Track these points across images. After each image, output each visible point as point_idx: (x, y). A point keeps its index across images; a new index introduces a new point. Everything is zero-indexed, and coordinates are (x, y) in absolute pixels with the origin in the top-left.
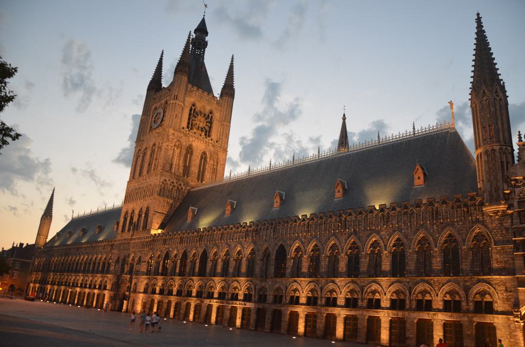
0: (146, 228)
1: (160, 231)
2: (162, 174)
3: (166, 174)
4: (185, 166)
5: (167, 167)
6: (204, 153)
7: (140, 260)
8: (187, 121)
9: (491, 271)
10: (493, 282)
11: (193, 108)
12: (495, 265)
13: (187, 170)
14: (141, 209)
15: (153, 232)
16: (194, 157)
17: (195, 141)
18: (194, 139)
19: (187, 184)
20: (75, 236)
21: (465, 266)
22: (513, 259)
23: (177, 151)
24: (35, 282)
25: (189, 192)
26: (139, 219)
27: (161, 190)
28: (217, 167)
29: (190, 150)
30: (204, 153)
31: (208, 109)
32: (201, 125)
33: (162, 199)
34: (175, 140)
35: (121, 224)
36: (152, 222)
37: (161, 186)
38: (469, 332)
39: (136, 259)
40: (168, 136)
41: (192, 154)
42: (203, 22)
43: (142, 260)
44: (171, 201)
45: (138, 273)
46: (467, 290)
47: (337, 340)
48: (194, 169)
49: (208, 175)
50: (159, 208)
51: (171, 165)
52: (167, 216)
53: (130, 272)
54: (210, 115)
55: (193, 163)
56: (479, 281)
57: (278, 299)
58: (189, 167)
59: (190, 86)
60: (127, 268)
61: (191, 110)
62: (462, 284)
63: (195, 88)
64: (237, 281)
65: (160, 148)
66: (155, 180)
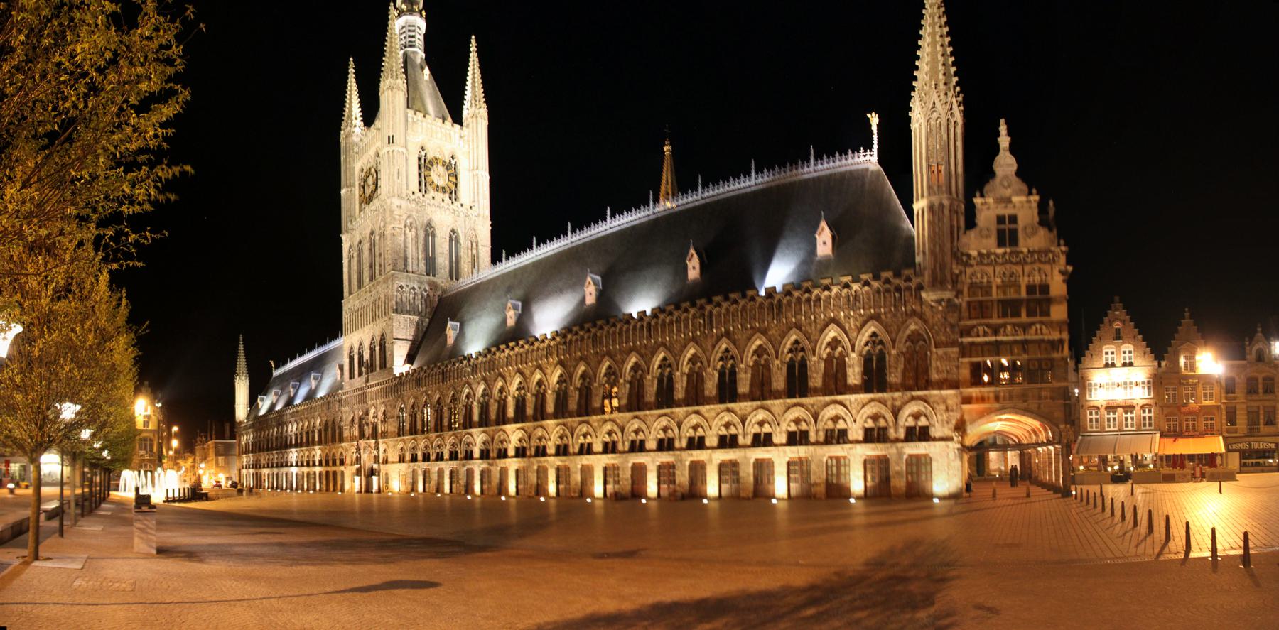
0: (385, 363)
1: (407, 368)
3: (400, 275)
5: (400, 265)
9: (928, 385)
10: (931, 400)
12: (935, 376)
15: (397, 372)
21: (894, 377)
22: (957, 367)
23: (411, 235)
25: (440, 299)
26: (371, 355)
29: (429, 231)
33: (401, 317)
34: (405, 217)
35: (346, 368)
36: (392, 355)
38: (897, 468)
39: (380, 415)
40: (392, 212)
41: (434, 235)
43: (388, 414)
44: (416, 318)
46: (896, 412)
47: (709, 499)
48: (442, 261)
49: (465, 266)
51: (406, 260)
55: (438, 250)
56: (913, 398)
58: (434, 258)
62: (889, 403)
64: (542, 427)
65: (382, 235)
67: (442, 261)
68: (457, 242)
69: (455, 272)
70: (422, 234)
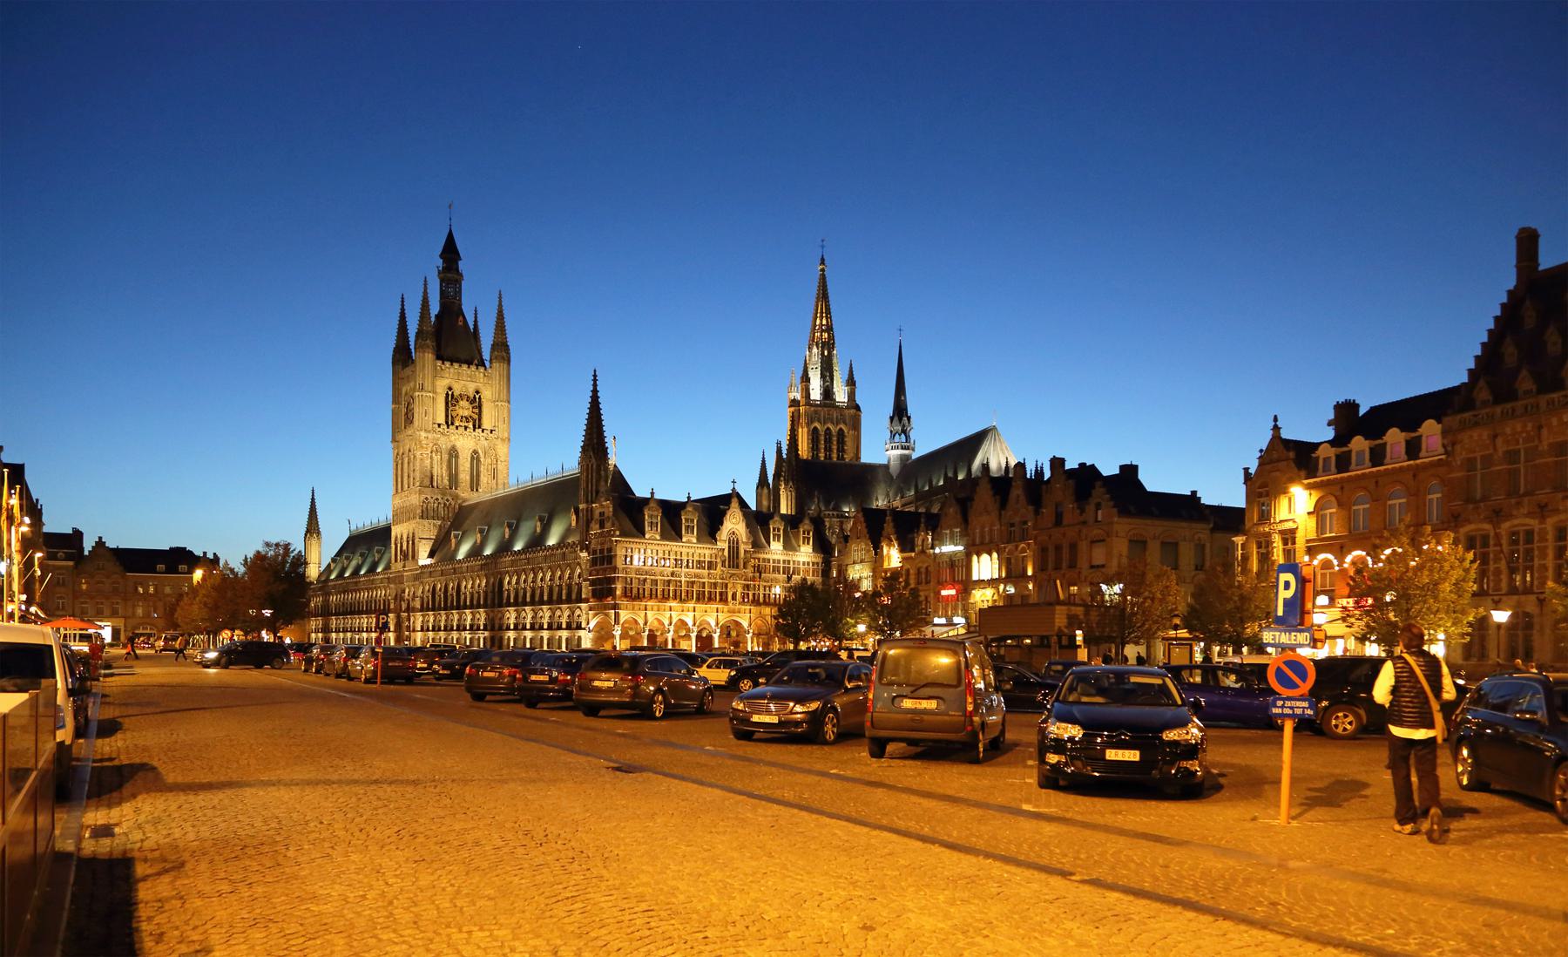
1: (429, 561)
2: (421, 493)
4: (450, 475)
5: (427, 482)
6: (475, 452)
7: (414, 596)
13: (454, 479)
16: (461, 461)
19: (456, 497)
20: (354, 563)
23: (436, 458)
24: (317, 631)
29: (453, 453)
30: (475, 452)
31: (471, 388)
32: (466, 413)
33: (426, 522)
41: (457, 457)
45: (414, 610)
48: (464, 476)
49: (485, 479)
50: (427, 532)
52: (436, 541)
53: (408, 610)
57: (501, 628)
58: (457, 474)
59: (439, 363)
60: (404, 606)
63: (448, 364)
66: (415, 499)
67: (464, 476)
68: (478, 459)
69: (475, 484)
70: (446, 457)
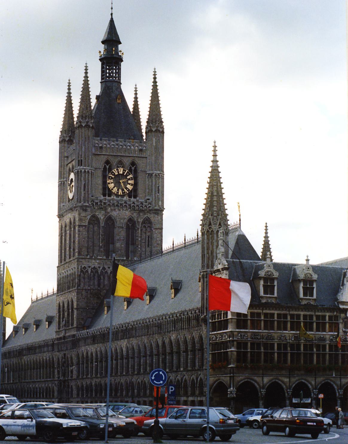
8: (101, 187)
11: (108, 167)
14: (69, 303)
16: (116, 231)
17: (115, 210)
18: (112, 208)
27: (80, 280)
28: (152, 234)
30: (131, 220)
34: (89, 217)
37: (80, 275)
42: (112, 22)
54: (133, 168)
61: (105, 168)
